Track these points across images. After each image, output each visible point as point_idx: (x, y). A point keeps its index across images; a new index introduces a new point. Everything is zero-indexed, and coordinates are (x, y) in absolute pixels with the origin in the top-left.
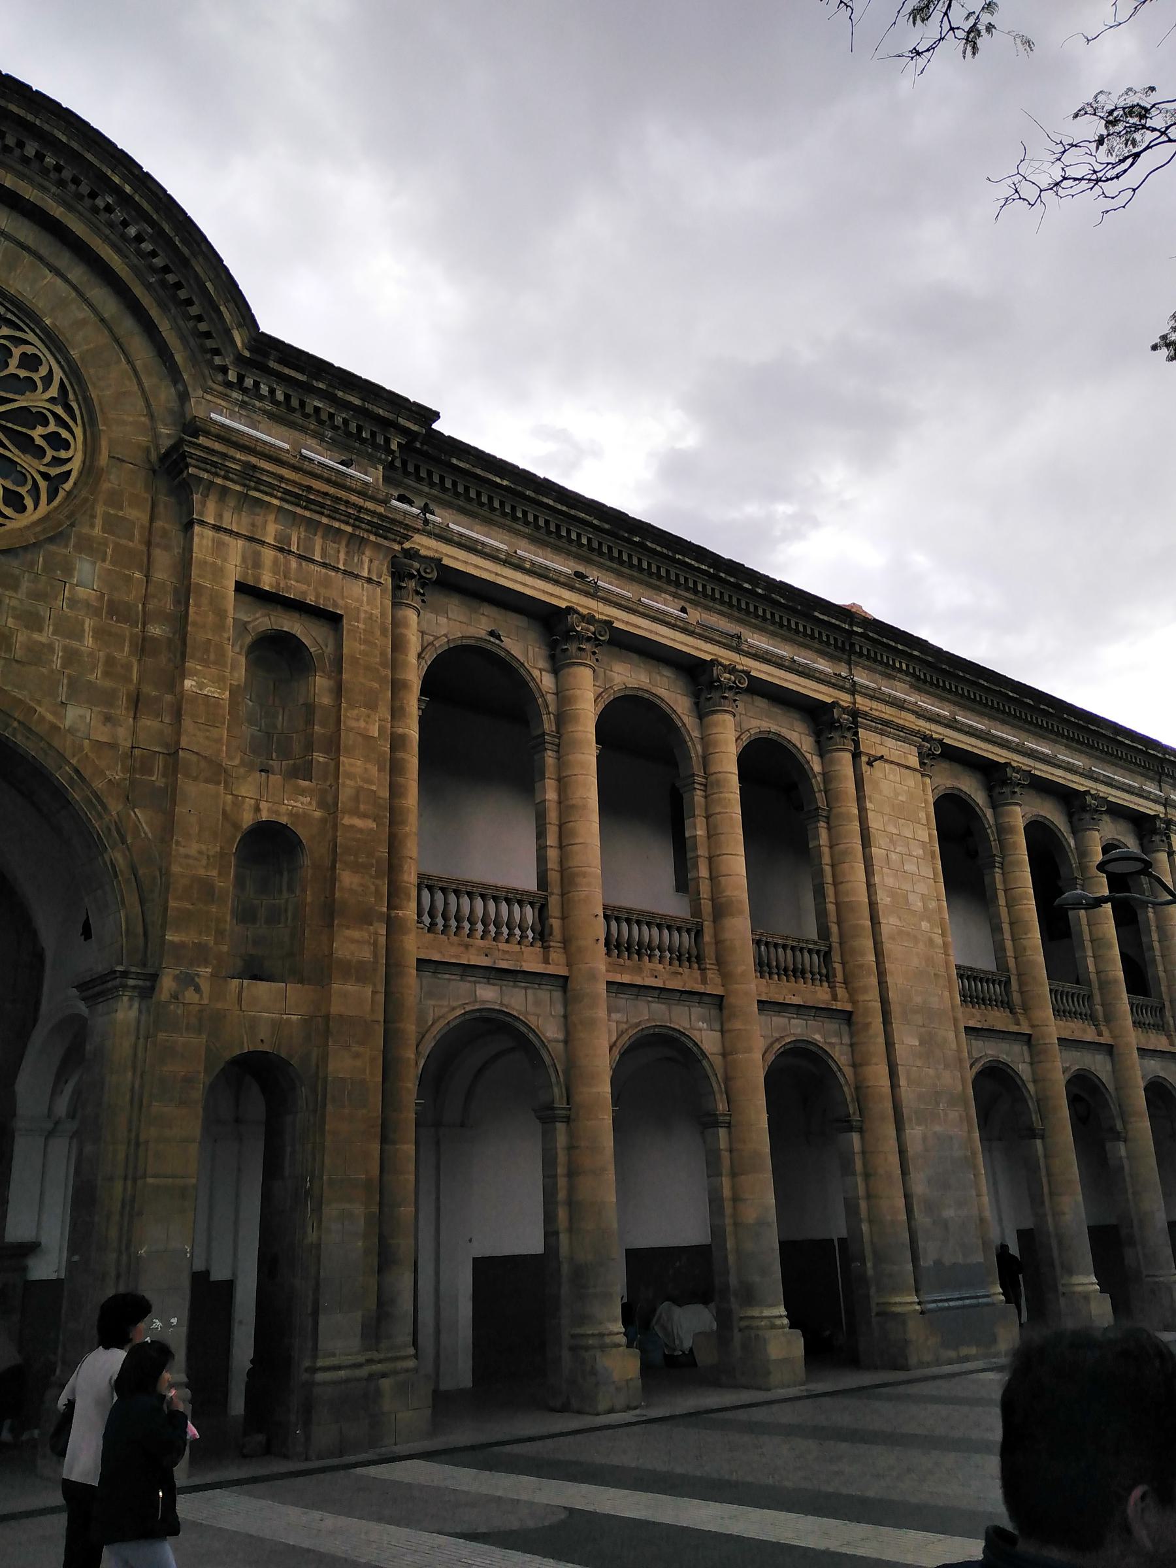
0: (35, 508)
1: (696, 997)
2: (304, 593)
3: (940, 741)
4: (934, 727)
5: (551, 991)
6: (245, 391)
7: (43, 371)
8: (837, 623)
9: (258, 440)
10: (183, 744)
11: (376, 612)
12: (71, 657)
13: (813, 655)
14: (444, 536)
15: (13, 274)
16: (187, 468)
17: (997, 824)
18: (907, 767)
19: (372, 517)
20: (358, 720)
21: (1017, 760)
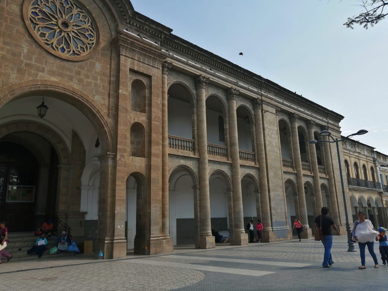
1: (227, 164)
4: (279, 104)
7: (87, 19)
8: (259, 80)
9: (133, 36)
10: (119, 105)
12: (96, 85)
16: (119, 42)
17: (291, 127)
18: (273, 113)
20: (155, 100)
21: (297, 112)
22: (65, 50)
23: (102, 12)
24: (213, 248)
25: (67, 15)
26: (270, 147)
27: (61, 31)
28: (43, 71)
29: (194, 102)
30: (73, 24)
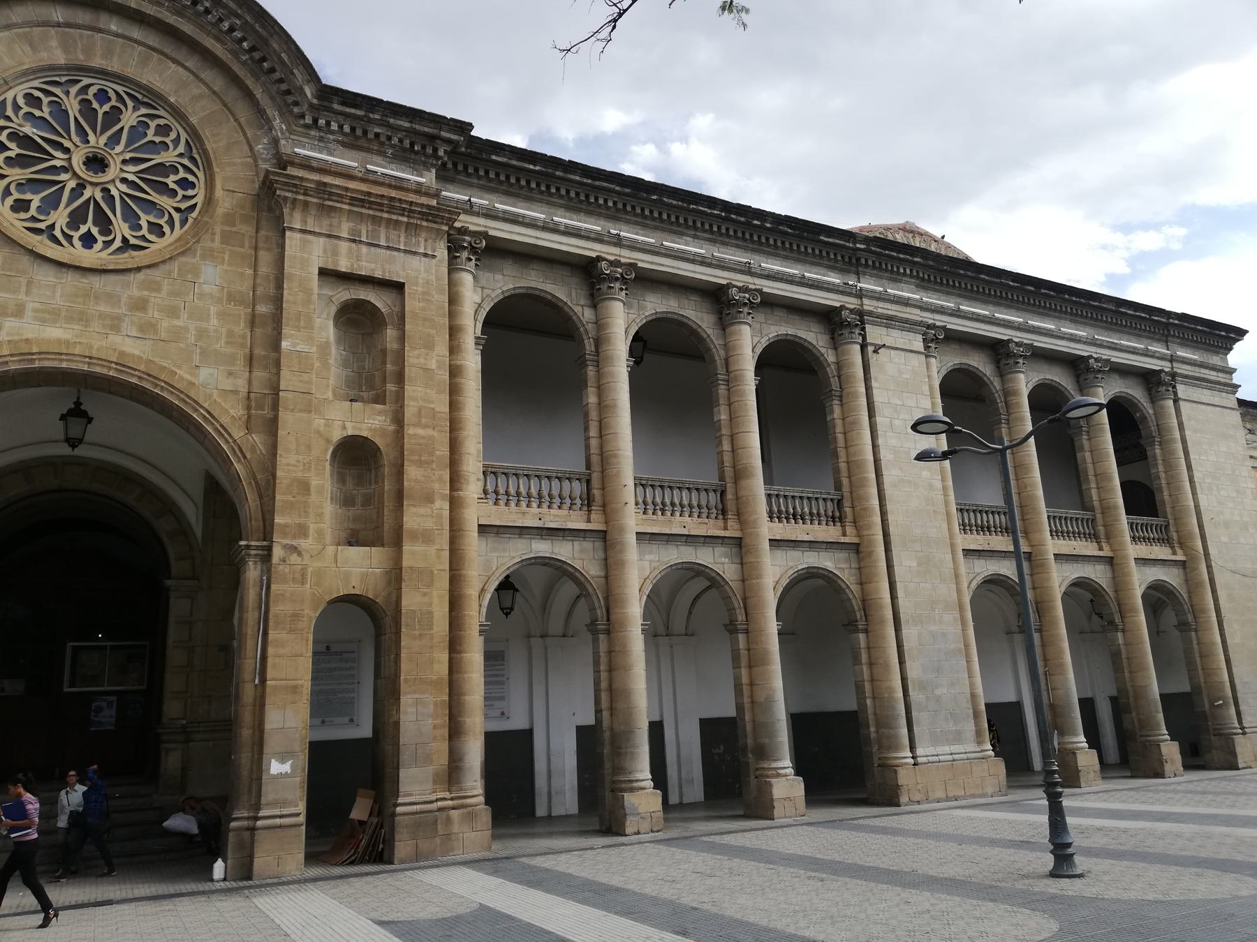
0: (172, 232)
2: (373, 270)
3: (944, 328)
4: (937, 317)
5: (594, 541)
6: (319, 129)
7: (173, 135)
8: (842, 242)
11: (433, 278)
13: (823, 271)
14: (490, 214)
15: (146, 70)
17: (1004, 390)
18: (912, 351)
19: (422, 208)
20: (417, 358)
21: (1017, 336)
22: (95, 241)
23: (225, 106)
24: (652, 831)
25: (102, 132)
26: (901, 469)
27: (81, 186)
28: (19, 312)
29: (587, 347)
30: (121, 158)
